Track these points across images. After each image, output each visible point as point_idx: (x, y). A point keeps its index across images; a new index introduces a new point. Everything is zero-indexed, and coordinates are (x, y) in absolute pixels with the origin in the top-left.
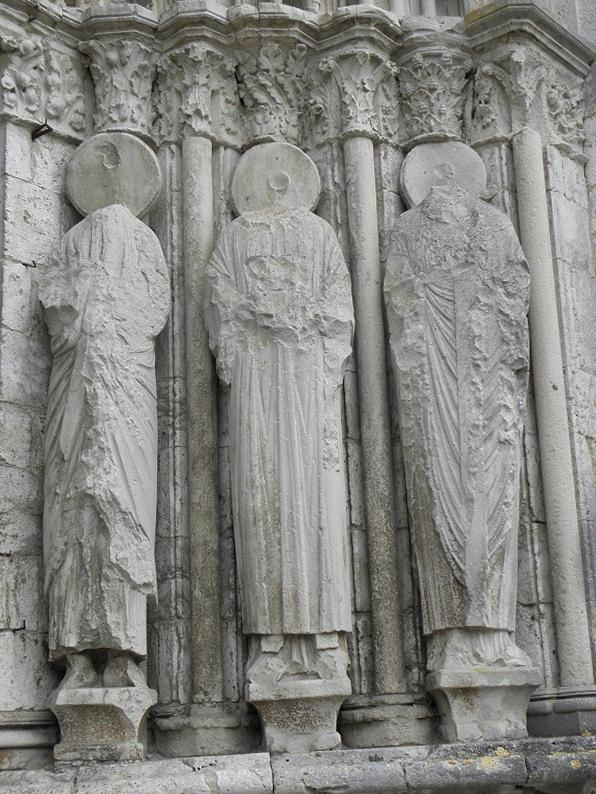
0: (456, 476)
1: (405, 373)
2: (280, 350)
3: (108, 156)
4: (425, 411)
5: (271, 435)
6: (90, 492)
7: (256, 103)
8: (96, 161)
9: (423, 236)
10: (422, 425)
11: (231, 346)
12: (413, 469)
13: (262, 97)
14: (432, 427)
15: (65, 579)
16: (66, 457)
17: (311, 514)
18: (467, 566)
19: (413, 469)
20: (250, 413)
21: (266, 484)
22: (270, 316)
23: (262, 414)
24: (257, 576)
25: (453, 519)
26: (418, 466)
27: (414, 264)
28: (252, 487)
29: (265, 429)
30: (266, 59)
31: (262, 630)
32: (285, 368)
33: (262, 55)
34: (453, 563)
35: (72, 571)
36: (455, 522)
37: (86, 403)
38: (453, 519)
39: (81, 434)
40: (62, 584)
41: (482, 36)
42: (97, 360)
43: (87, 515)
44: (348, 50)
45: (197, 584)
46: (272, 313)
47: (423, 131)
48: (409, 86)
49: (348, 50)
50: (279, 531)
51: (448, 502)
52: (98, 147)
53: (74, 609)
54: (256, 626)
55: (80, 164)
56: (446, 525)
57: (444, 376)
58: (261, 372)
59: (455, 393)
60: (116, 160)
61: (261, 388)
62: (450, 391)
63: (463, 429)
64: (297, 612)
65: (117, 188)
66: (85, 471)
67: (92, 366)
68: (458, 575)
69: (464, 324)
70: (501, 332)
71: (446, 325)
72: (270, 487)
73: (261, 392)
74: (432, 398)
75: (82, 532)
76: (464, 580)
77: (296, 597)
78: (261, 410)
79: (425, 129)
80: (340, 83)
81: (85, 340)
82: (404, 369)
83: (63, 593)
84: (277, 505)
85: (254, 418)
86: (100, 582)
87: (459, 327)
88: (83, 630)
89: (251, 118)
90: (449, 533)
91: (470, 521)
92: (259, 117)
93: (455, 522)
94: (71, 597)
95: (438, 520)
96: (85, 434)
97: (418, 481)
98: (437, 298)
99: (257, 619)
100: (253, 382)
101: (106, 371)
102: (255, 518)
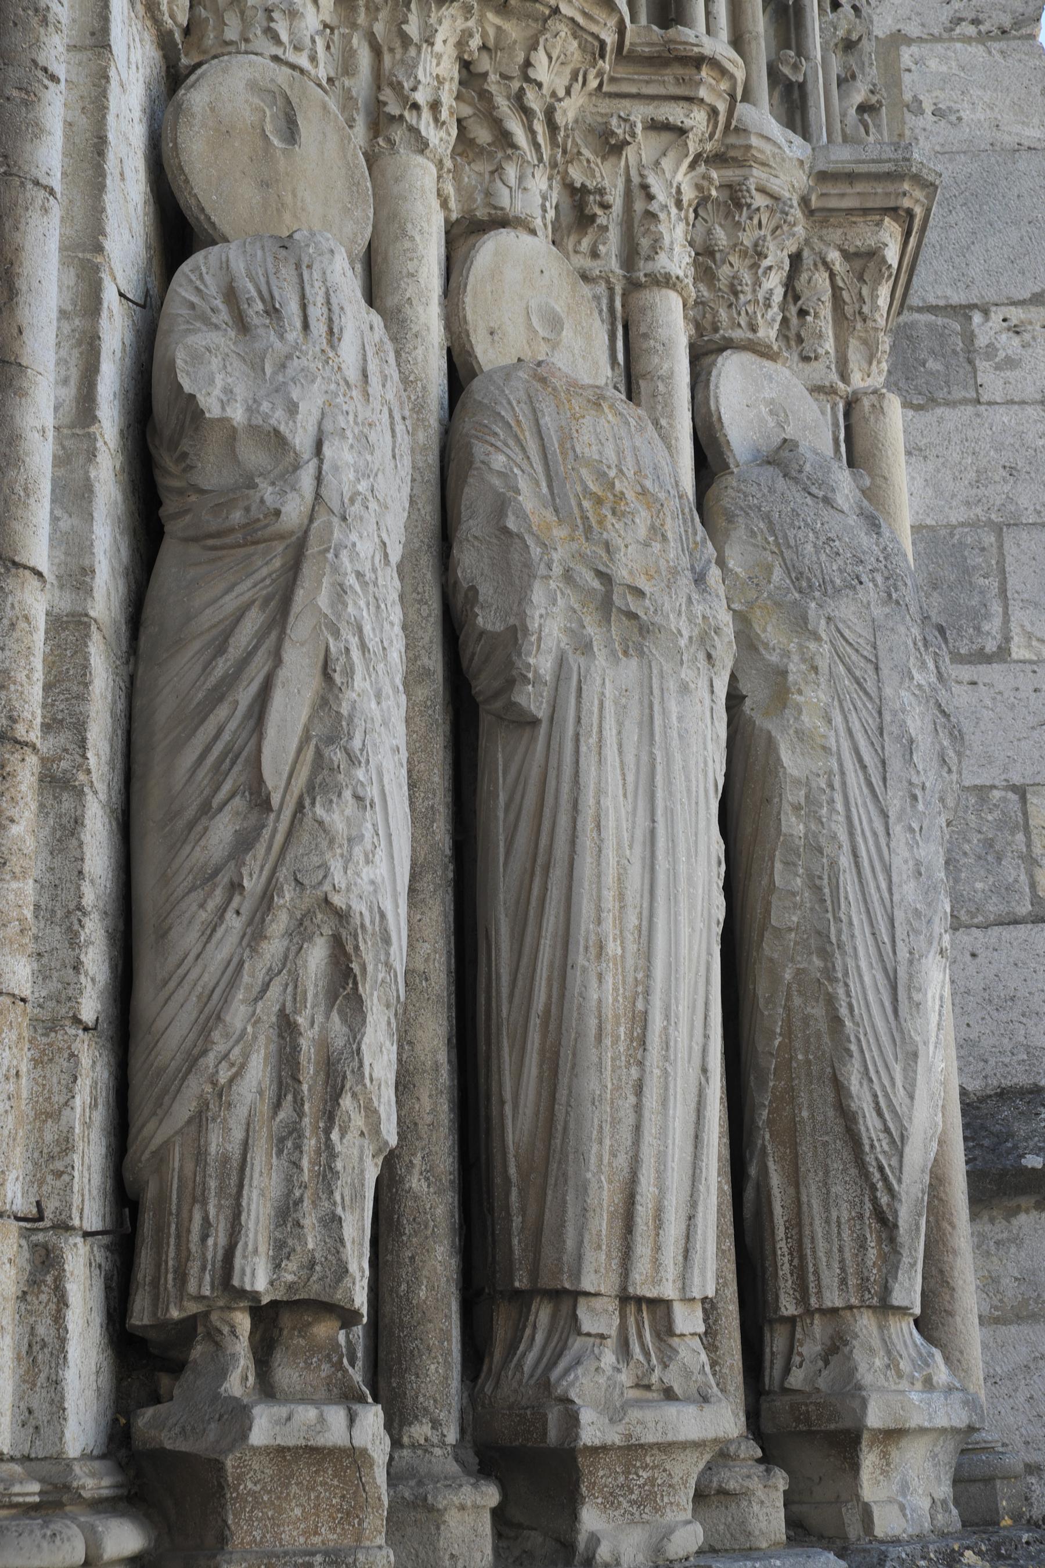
0: (887, 1004)
1: (797, 782)
2: (655, 671)
3: (272, 116)
4: (833, 864)
5: (638, 849)
6: (337, 900)
7: (505, 138)
8: (249, 117)
9: (807, 525)
10: (827, 890)
11: (550, 634)
12: (788, 976)
13: (520, 137)
14: (846, 898)
15: (241, 1112)
16: (275, 800)
17: (691, 1040)
18: (904, 1186)
19: (788, 976)
20: (600, 792)
21: (623, 956)
22: (640, 593)
23: (621, 798)
24: (593, 1160)
25: (883, 1087)
26: (799, 972)
27: (797, 576)
28: (599, 955)
29: (626, 835)
30: (545, 59)
31: (588, 1284)
32: (665, 712)
33: (541, 48)
34: (877, 1175)
35: (261, 1093)
36: (886, 1095)
37: (327, 674)
38: (883, 1087)
39: (309, 754)
40: (232, 1123)
41: (842, 195)
42: (351, 580)
43: (316, 957)
44: (675, 113)
45: (417, 1161)
46: (647, 589)
47: (739, 325)
48: (721, 236)
49: (675, 113)
50: (641, 1064)
51: (876, 1054)
52: (253, 86)
53: (262, 1194)
54: (577, 1274)
55: (213, 110)
56: (869, 1098)
57: (865, 804)
58: (622, 710)
59: (883, 841)
60: (291, 131)
61: (620, 745)
62: (875, 834)
63: (899, 916)
64: (657, 1248)
65: (289, 199)
66: (324, 844)
67: (341, 591)
68: (884, 1200)
69: (894, 713)
70: (941, 744)
71: (864, 705)
72: (630, 962)
73: (620, 753)
74: (846, 847)
75: (298, 997)
76: (896, 1213)
77: (659, 1213)
78: (621, 792)
79: (742, 323)
80: (633, 173)
81: (329, 527)
82: (795, 773)
83: (234, 1149)
84: (640, 1006)
85: (608, 802)
86: (328, 1131)
87: (887, 717)
88: (280, 1252)
89: (483, 167)
90: (874, 1114)
91: (912, 1097)
92: (511, 172)
93: (886, 1095)
94: (259, 1158)
95: (855, 1084)
96: (319, 754)
97: (797, 1001)
98: (848, 649)
99: (580, 1258)
100: (606, 726)
101: (365, 613)
102: (600, 1028)
